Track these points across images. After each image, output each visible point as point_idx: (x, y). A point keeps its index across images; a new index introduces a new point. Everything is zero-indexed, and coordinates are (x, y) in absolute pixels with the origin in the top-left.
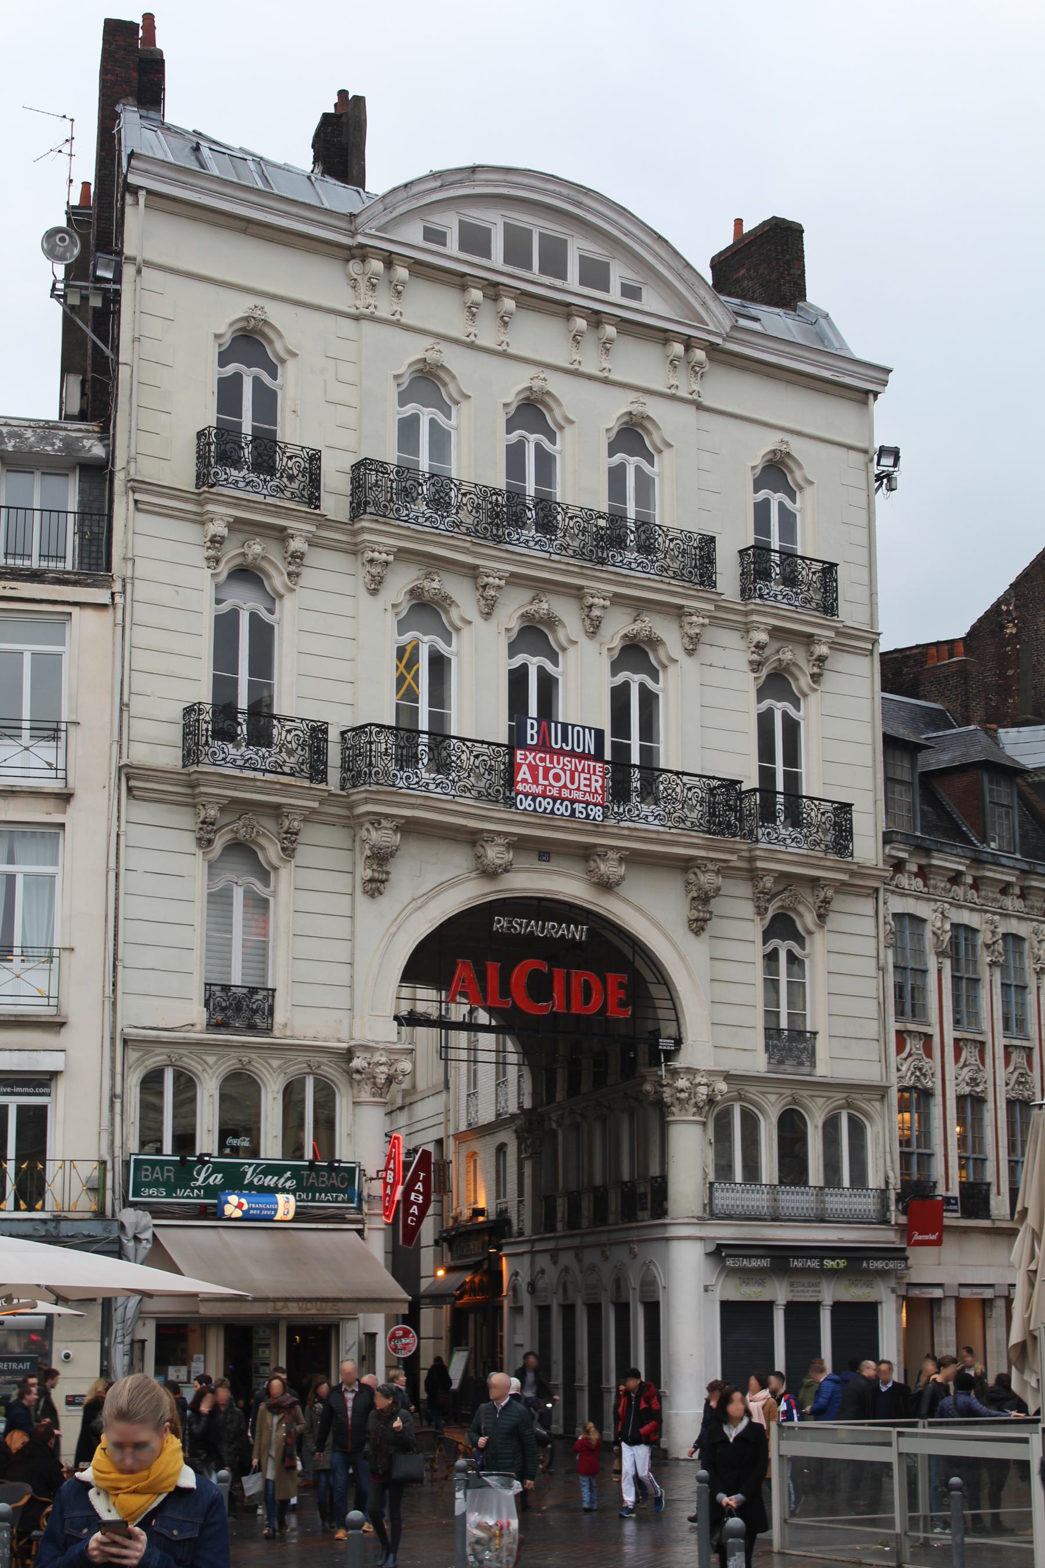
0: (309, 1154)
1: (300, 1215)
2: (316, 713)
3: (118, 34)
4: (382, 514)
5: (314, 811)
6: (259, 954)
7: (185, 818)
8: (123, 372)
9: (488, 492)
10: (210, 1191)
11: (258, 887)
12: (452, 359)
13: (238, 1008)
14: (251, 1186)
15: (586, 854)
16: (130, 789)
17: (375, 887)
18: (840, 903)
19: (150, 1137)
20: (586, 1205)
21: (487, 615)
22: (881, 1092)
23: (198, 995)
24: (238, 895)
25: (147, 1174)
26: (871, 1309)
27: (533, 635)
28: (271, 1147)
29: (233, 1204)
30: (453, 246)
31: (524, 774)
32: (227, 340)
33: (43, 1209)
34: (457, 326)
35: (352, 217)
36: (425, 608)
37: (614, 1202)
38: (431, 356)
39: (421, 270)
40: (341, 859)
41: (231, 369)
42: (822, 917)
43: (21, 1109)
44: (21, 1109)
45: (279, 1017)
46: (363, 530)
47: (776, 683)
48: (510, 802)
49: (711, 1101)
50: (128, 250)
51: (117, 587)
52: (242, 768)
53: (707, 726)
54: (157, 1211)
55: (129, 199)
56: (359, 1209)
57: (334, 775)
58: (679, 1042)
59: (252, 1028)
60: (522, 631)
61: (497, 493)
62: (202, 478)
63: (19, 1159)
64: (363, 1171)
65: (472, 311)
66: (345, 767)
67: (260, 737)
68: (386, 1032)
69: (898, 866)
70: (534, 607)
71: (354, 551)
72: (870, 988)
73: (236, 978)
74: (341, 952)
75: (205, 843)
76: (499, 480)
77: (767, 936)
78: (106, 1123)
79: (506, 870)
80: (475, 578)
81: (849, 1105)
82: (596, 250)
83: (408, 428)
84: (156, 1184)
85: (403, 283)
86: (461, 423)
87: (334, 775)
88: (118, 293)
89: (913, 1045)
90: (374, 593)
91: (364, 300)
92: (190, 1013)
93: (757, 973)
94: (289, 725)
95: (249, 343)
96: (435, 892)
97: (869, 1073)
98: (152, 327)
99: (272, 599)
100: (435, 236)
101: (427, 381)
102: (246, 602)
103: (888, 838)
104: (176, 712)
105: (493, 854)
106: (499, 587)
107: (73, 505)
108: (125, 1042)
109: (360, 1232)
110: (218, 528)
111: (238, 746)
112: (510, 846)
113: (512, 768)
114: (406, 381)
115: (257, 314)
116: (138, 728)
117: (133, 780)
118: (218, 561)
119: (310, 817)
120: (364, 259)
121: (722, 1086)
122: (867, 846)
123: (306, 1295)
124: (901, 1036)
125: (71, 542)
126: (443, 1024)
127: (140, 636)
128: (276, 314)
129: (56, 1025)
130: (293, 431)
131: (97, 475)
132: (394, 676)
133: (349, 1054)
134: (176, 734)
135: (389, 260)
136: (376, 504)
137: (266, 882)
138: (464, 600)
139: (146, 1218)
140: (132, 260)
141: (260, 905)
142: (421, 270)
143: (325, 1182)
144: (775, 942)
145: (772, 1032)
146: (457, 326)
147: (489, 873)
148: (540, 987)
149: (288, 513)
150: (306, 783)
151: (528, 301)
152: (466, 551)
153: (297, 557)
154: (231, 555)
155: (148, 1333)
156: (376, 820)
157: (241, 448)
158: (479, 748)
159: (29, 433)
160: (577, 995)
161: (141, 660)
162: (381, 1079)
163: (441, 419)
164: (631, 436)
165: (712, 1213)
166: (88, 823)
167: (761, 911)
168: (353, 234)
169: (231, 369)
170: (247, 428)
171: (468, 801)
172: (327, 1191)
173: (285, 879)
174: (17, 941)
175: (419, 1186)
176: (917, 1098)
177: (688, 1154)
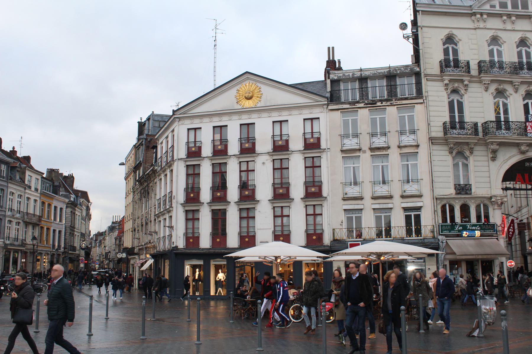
0: (483, 221)
1: (481, 236)
2: (474, 120)
4: (486, 72)
5: (476, 143)
6: (467, 176)
7: (446, 148)
8: (421, 51)
9: (513, 63)
10: (459, 231)
11: (465, 161)
12: (500, 34)
13: (463, 189)
14: (469, 229)
16: (432, 143)
17: (494, 159)
19: (444, 220)
21: (516, 92)
23: (453, 187)
24: (460, 164)
25: (444, 228)
28: (474, 220)
29: (465, 234)
30: (498, 8)
31: (529, 128)
32: (444, 40)
33: (421, 236)
34: (501, 26)
35: (471, 6)
36: (500, 93)
38: (495, 34)
39: (490, 15)
40: (485, 153)
41: (446, 46)
43: (414, 215)
44: (414, 215)
45: (473, 191)
46: (482, 77)
48: (526, 135)
50: (419, 24)
51: (424, 98)
52: (458, 135)
54: (447, 236)
55: (418, 13)
56: (497, 233)
57: (481, 134)
59: (467, 194)
60: (526, 95)
61: (515, 63)
62: (441, 71)
63: (415, 226)
64: (497, 225)
65: (504, 22)
66: (483, 132)
67: (462, 128)
68: (500, 192)
70: (528, 89)
71: (480, 82)
73: (462, 183)
74: (487, 174)
75: (451, 153)
76: (516, 60)
78: (433, 217)
79: (527, 151)
80: (512, 84)
83: (491, 53)
84: (446, 230)
85: (486, 19)
86: (504, 49)
87: (481, 134)
88: (418, 34)
90: (486, 91)
91: (476, 25)
92: (451, 191)
94: (468, 124)
95: (450, 39)
96: (509, 159)
98: (426, 40)
99: (462, 96)
100: (493, 6)
101: (495, 40)
102: (455, 98)
104: (441, 124)
105: (523, 148)
106: (518, 85)
107: (414, 82)
108: (436, 199)
109: (497, 239)
110: (446, 82)
111: (456, 130)
112: (527, 146)
113: (526, 127)
114: (489, 41)
115: (451, 33)
116: (433, 129)
117: (432, 141)
118: (447, 89)
119: (476, 144)
120: (475, 15)
123: (482, 253)
125: (415, 90)
126: (514, 189)
127: (431, 108)
128: (455, 32)
129: (420, 196)
130: (462, 57)
131: (418, 75)
132: (494, 109)
133: (491, 198)
134: (442, 129)
135: (481, 14)
136: (484, 70)
137: (467, 160)
138: (510, 89)
139: (444, 238)
140: (420, 26)
141: (466, 166)
142: (490, 15)
143: (487, 228)
146: (501, 26)
147: (523, 153)
149: (463, 76)
150: (474, 137)
151: (519, 17)
152: (509, 78)
153: (466, 86)
154: (450, 87)
155: (447, 263)
156: (492, 143)
157: (451, 63)
158: (516, 123)
159: (402, 68)
161: (432, 114)
162: (499, 203)
163: (499, 48)
166: (423, 151)
168: (472, 10)
169: (446, 46)
170: (451, 58)
171: (515, 136)
172: (488, 230)
173: (471, 159)
174: (410, 179)
175: (512, 227)
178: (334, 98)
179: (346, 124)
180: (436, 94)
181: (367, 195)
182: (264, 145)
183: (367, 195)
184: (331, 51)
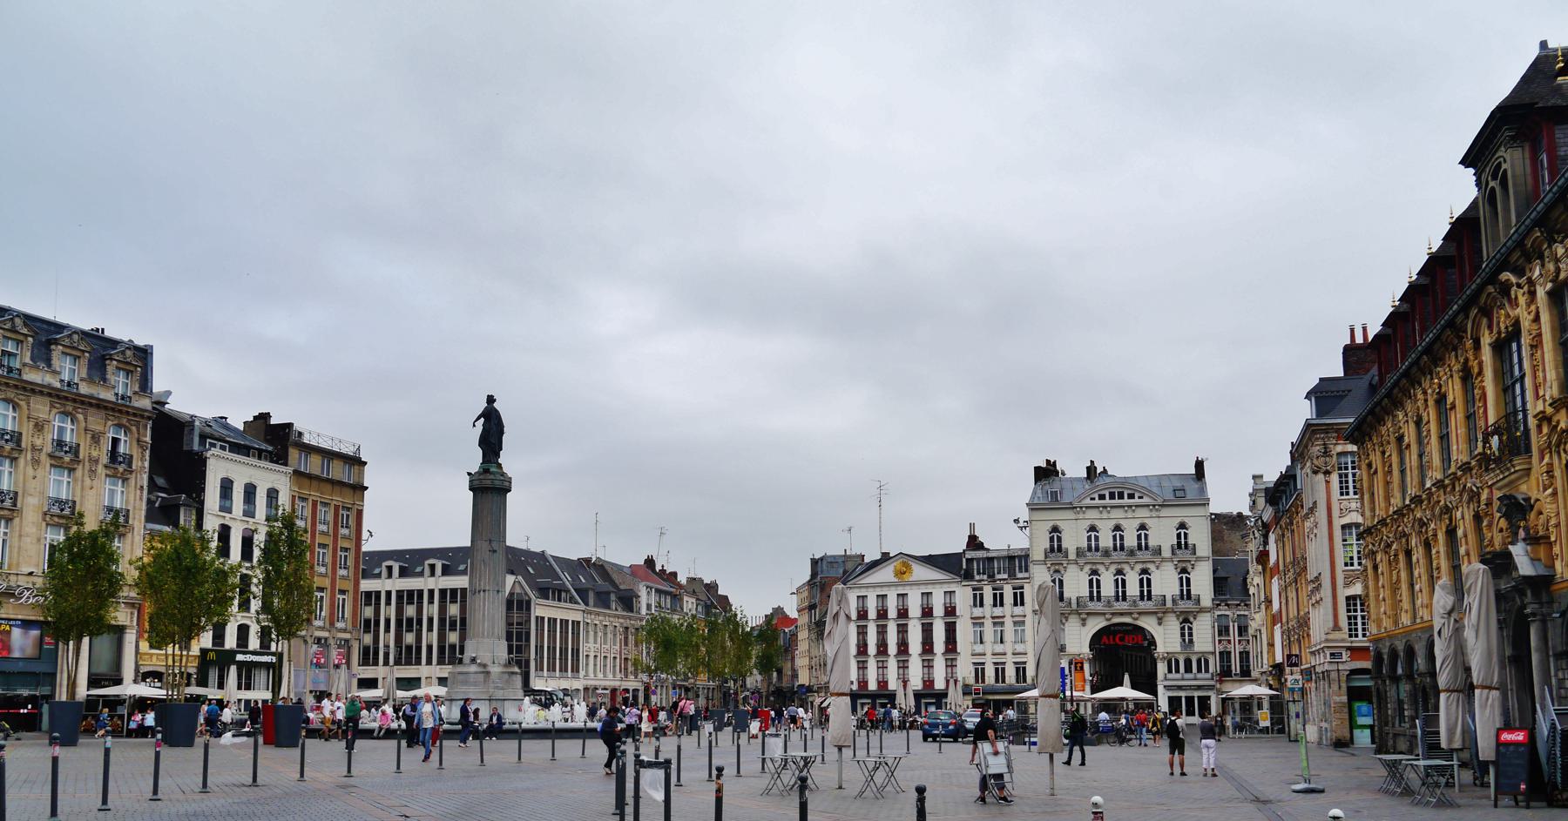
3: (1037, 469)
12: (1097, 523)
22: (1214, 653)
26: (1209, 698)
27: (1120, 572)
36: (1094, 572)
53: (1165, 582)
57: (1074, 606)
95: (1055, 529)
97: (1211, 649)
101: (1093, 528)
102: (1057, 576)
122: (1207, 601)
130: (1064, 545)
157: (1056, 548)
164: (1143, 527)
166: (1028, 620)
176: (1225, 656)
177: (1161, 668)
178: (968, 576)
180: (1040, 575)
181: (989, 653)
182: (915, 610)
183: (989, 653)
184: (972, 526)
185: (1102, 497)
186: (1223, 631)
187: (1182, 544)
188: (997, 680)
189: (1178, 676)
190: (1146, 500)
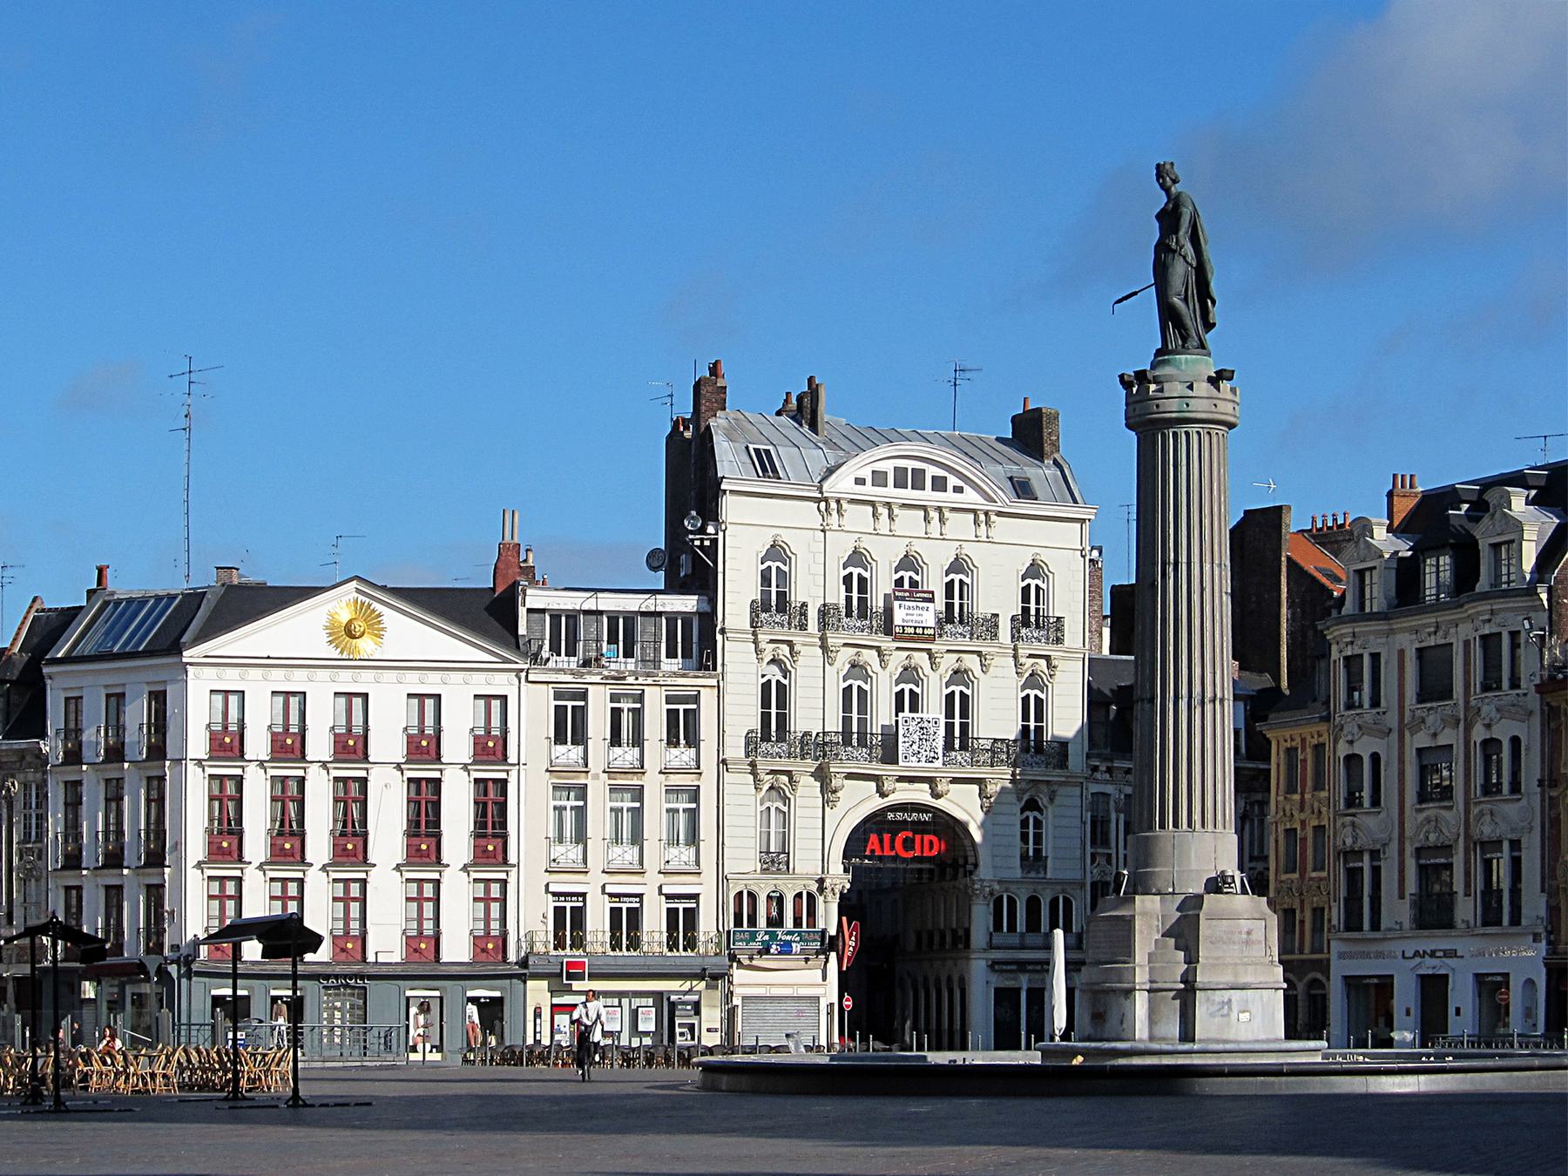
15: (931, 781)
18: (1062, 791)
20: (937, 939)
37: (948, 939)
42: (1051, 800)
47: (1033, 681)
49: (991, 894)
58: (976, 865)
69: (1095, 769)
72: (1077, 833)
77: (1022, 811)
81: (1063, 891)
82: (941, 473)
89: (1101, 860)
93: (1018, 830)
95: (776, 551)
97: (1078, 875)
101: (857, 557)
103: (1088, 756)
121: (997, 887)
122: (1076, 761)
124: (1093, 856)
130: (797, 596)
144: (1027, 813)
145: (1024, 856)
148: (908, 844)
160: (926, 848)
164: (957, 566)
165: (991, 946)
167: (1019, 799)
177: (980, 920)
179: (560, 712)
185: (879, 478)
186: (1099, 832)
187: (1033, 618)
188: (616, 944)
189: (1014, 940)
190: (970, 497)
